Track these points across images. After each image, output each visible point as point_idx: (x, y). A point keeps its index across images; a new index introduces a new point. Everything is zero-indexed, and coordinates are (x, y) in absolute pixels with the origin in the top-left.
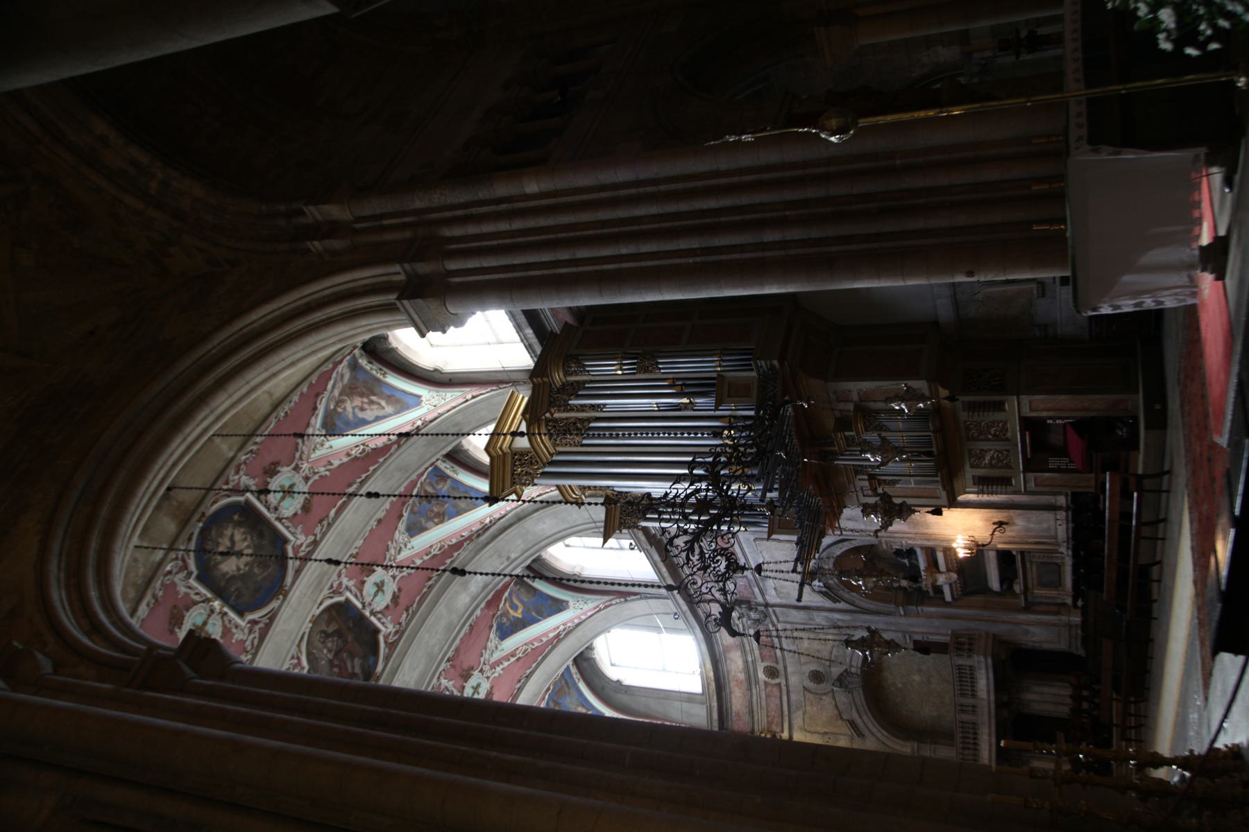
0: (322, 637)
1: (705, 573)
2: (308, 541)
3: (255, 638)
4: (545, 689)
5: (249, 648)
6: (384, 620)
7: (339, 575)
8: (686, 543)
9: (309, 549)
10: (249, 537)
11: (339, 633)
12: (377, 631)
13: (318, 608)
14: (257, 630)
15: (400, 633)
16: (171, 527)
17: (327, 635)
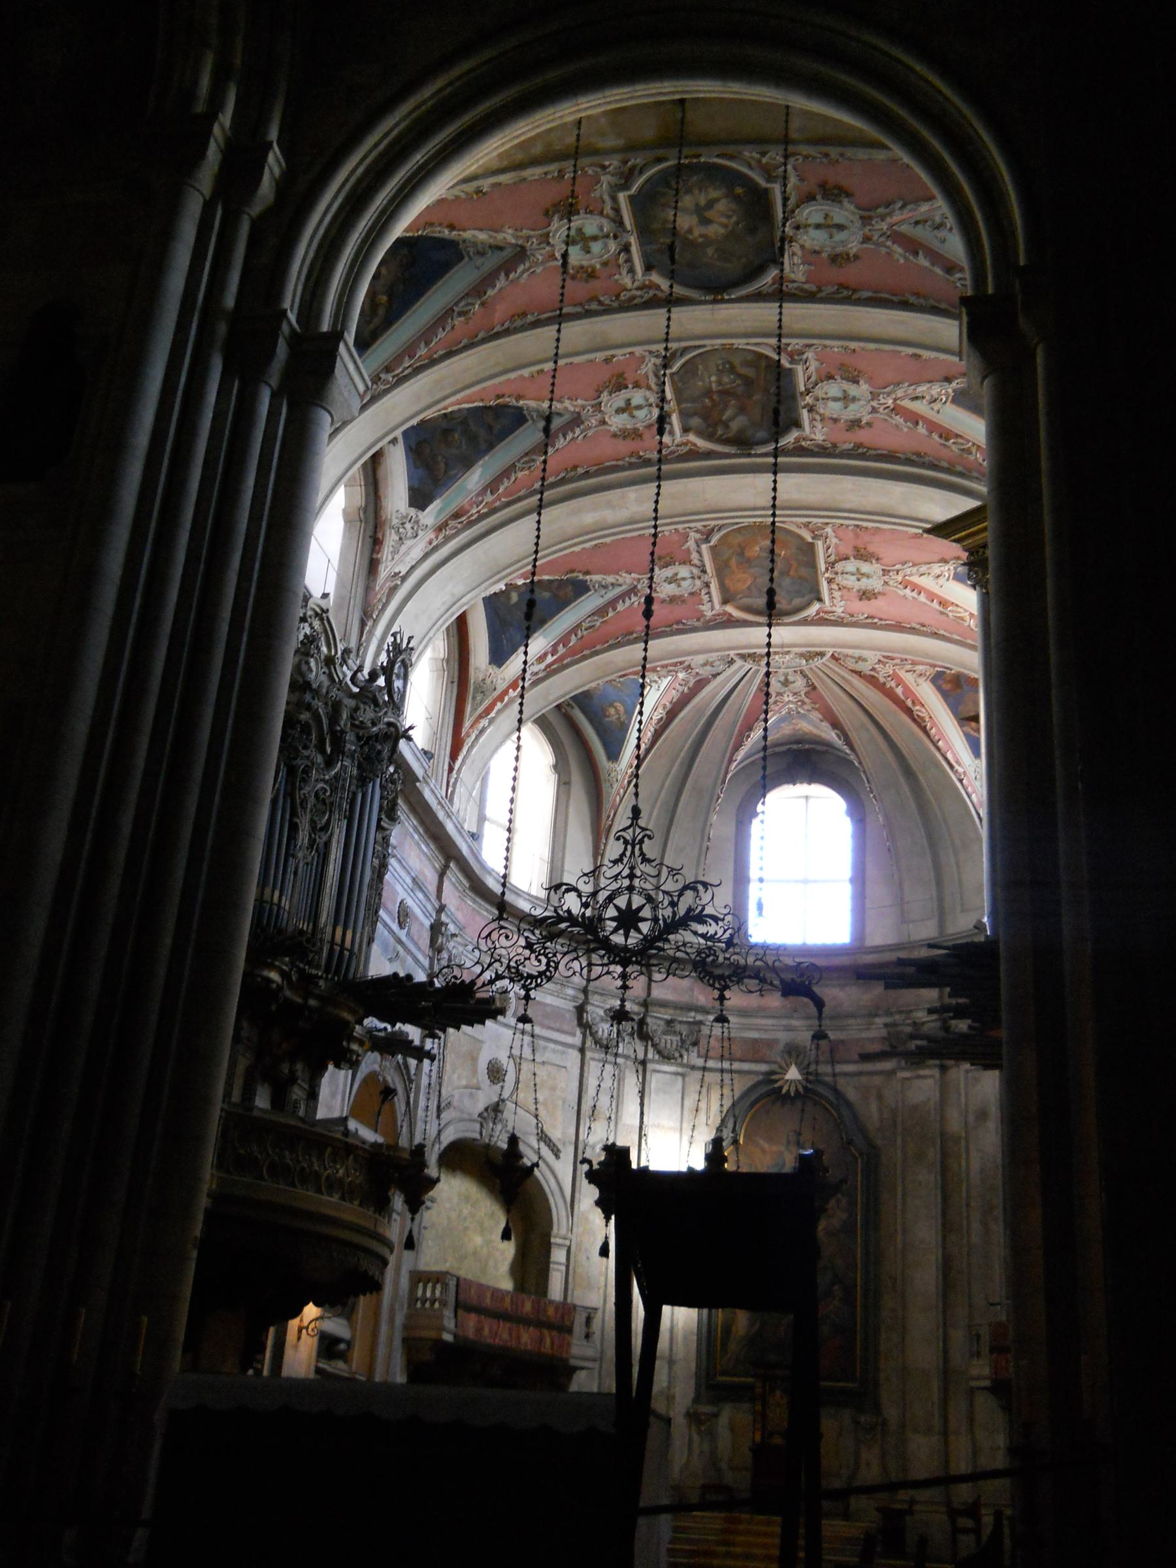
0: (724, 366)
1: (524, 948)
2: (806, 286)
3: (642, 297)
4: (949, 666)
5: (622, 298)
6: (815, 423)
7: (810, 346)
8: (569, 911)
9: (797, 292)
10: (735, 218)
11: (748, 382)
12: (798, 424)
13: (748, 344)
14: (651, 293)
15: (822, 451)
16: (649, 131)
17: (732, 370)
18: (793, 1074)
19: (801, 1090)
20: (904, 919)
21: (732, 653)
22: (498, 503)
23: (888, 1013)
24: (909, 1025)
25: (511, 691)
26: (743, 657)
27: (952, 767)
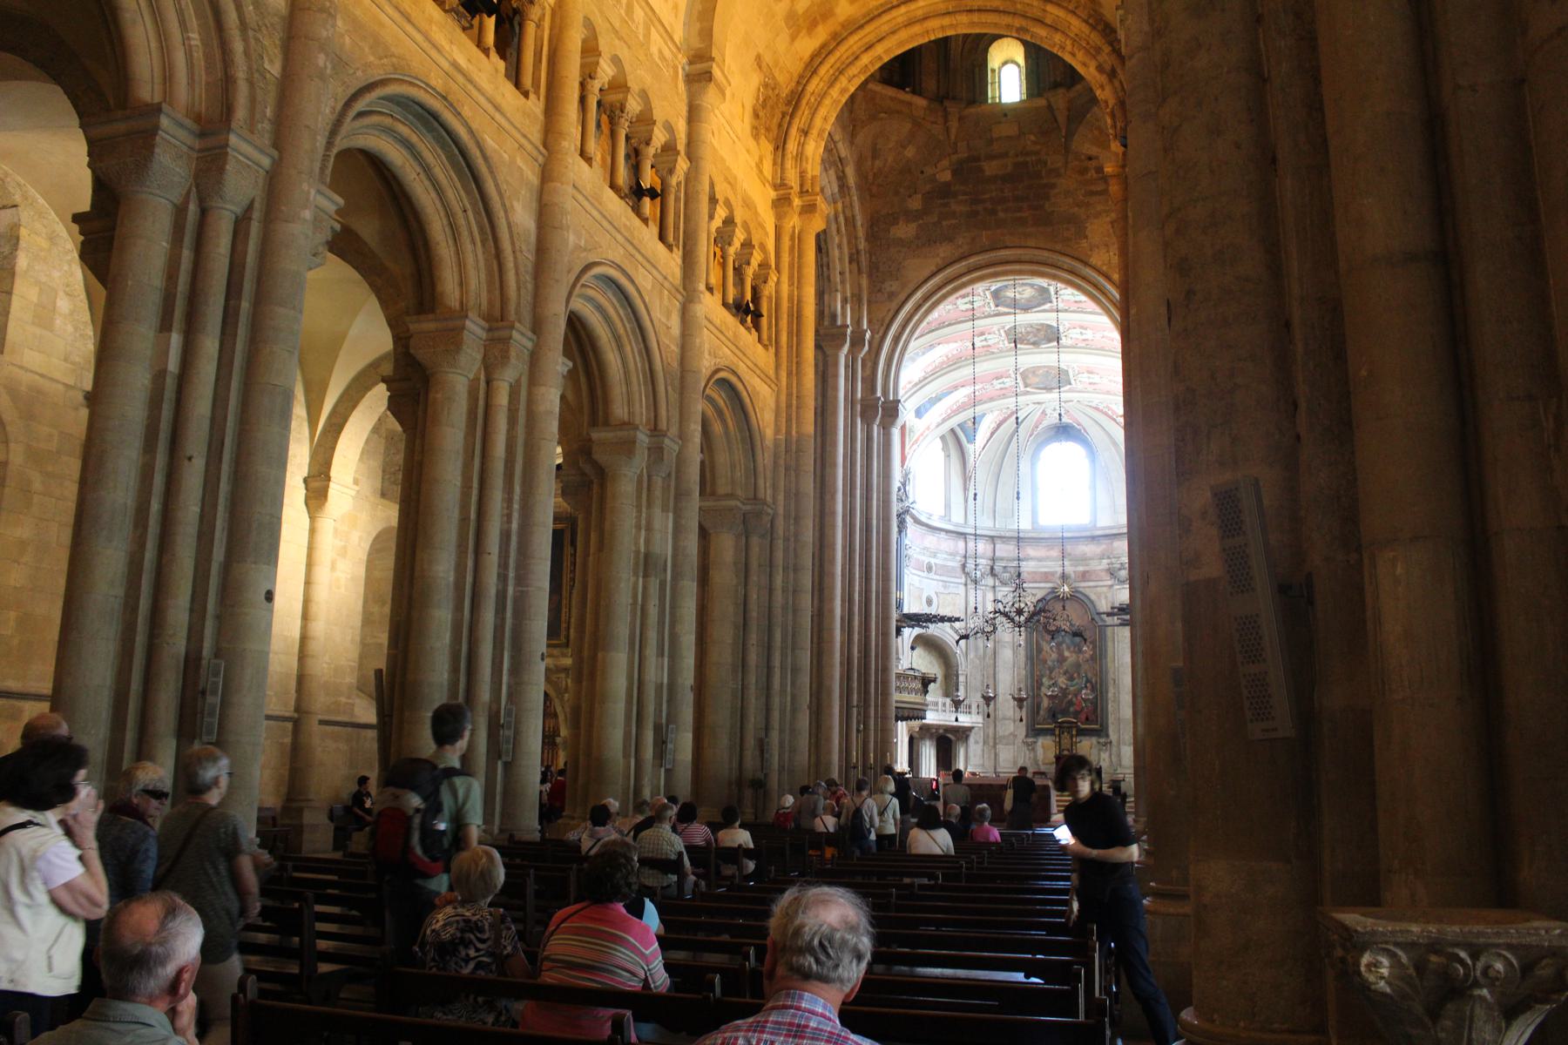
23: (1109, 558)
25: (927, 432)
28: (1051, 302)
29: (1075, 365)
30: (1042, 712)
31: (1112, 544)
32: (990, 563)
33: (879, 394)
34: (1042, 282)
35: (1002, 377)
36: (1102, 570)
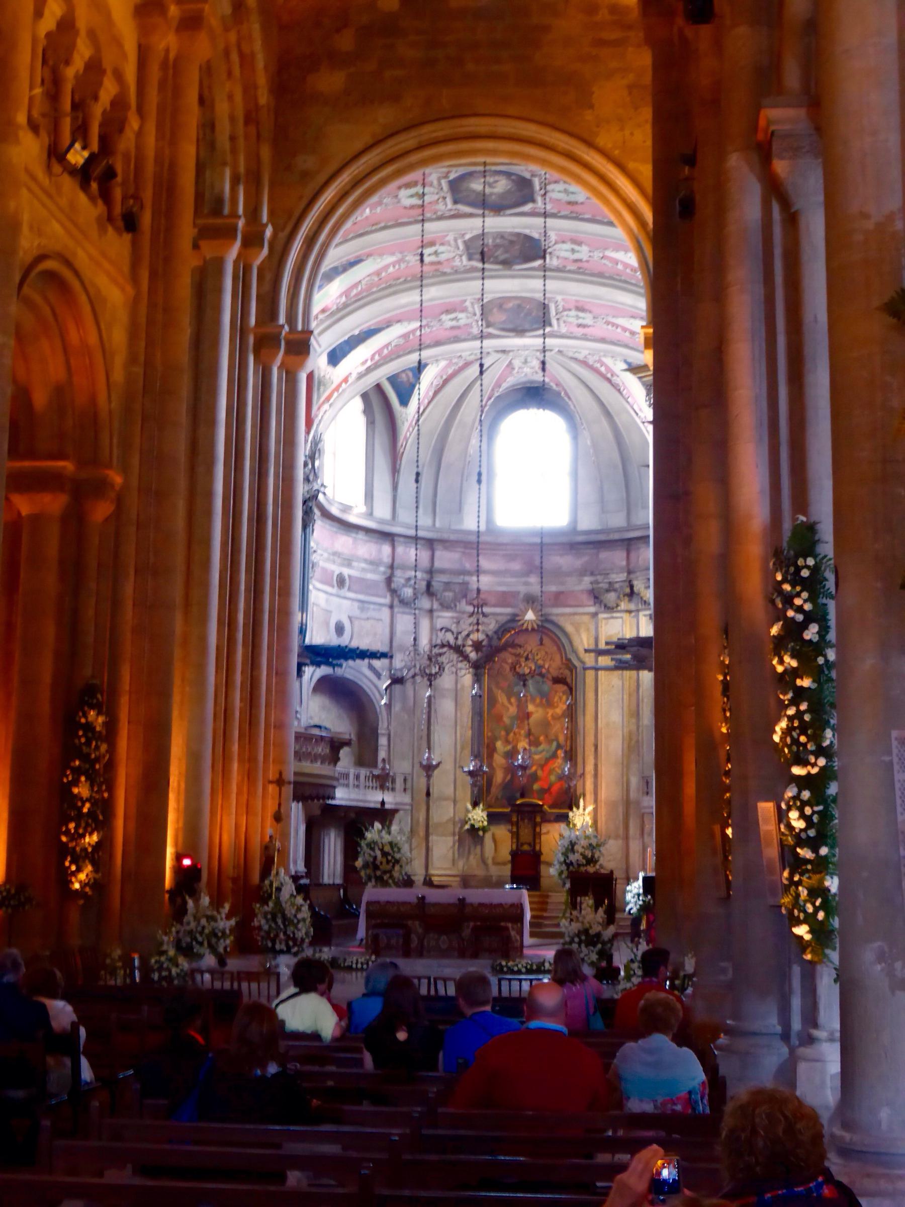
18: (530, 616)
19: (536, 627)
20: (603, 508)
21: (490, 350)
22: (349, 302)
23: (592, 574)
24: (606, 583)
25: (344, 385)
26: (497, 351)
27: (637, 414)
28: (533, 200)
29: (559, 298)
30: (493, 790)
31: (597, 555)
32: (426, 576)
33: (282, 320)
34: (524, 169)
35: (454, 311)
36: (582, 591)
